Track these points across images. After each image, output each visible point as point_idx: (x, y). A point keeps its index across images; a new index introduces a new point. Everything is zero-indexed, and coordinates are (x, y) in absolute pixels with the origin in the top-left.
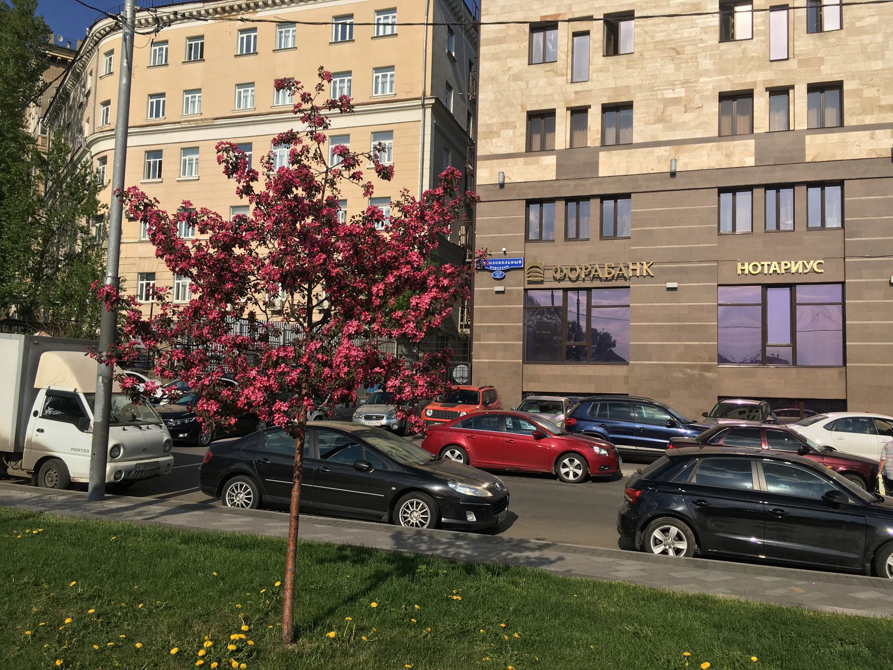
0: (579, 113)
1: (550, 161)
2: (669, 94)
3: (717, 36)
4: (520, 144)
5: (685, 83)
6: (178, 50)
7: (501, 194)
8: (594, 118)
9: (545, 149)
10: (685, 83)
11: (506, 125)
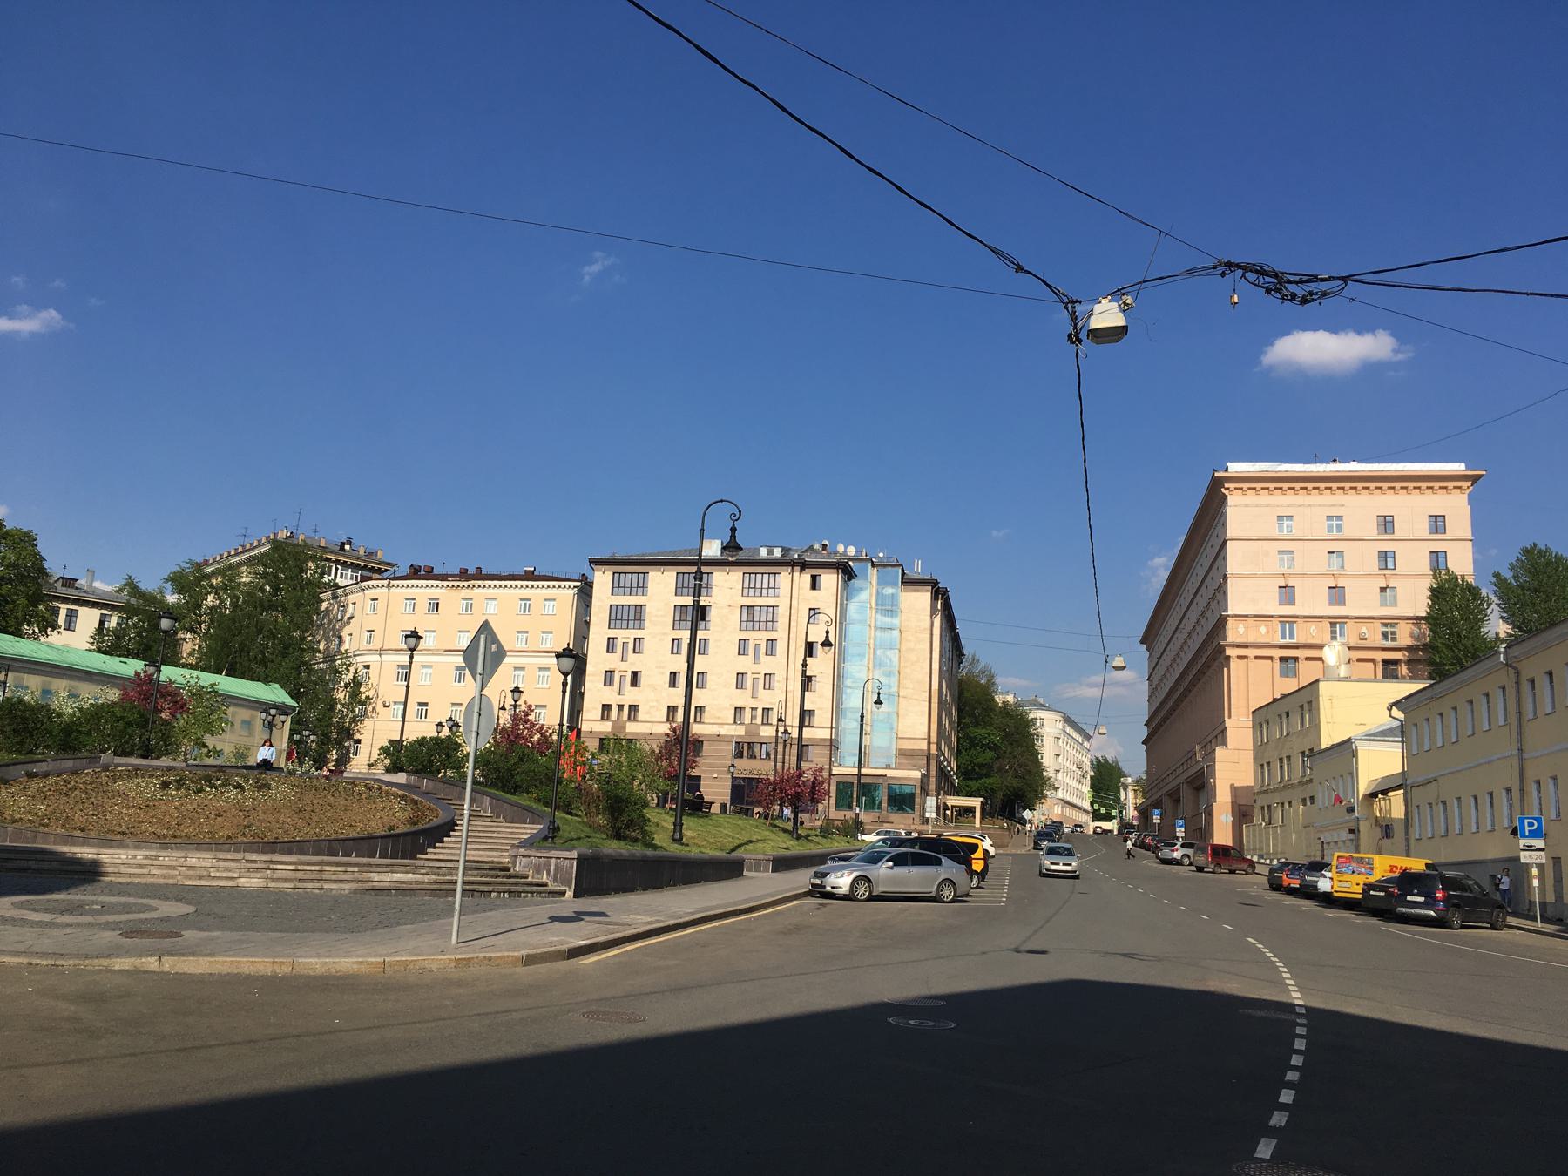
0: (621, 707)
1: (610, 724)
2: (651, 704)
3: (668, 685)
4: (599, 716)
5: (657, 701)
6: (422, 605)
7: (591, 735)
8: (626, 709)
9: (608, 719)
10: (657, 701)
11: (596, 709)
